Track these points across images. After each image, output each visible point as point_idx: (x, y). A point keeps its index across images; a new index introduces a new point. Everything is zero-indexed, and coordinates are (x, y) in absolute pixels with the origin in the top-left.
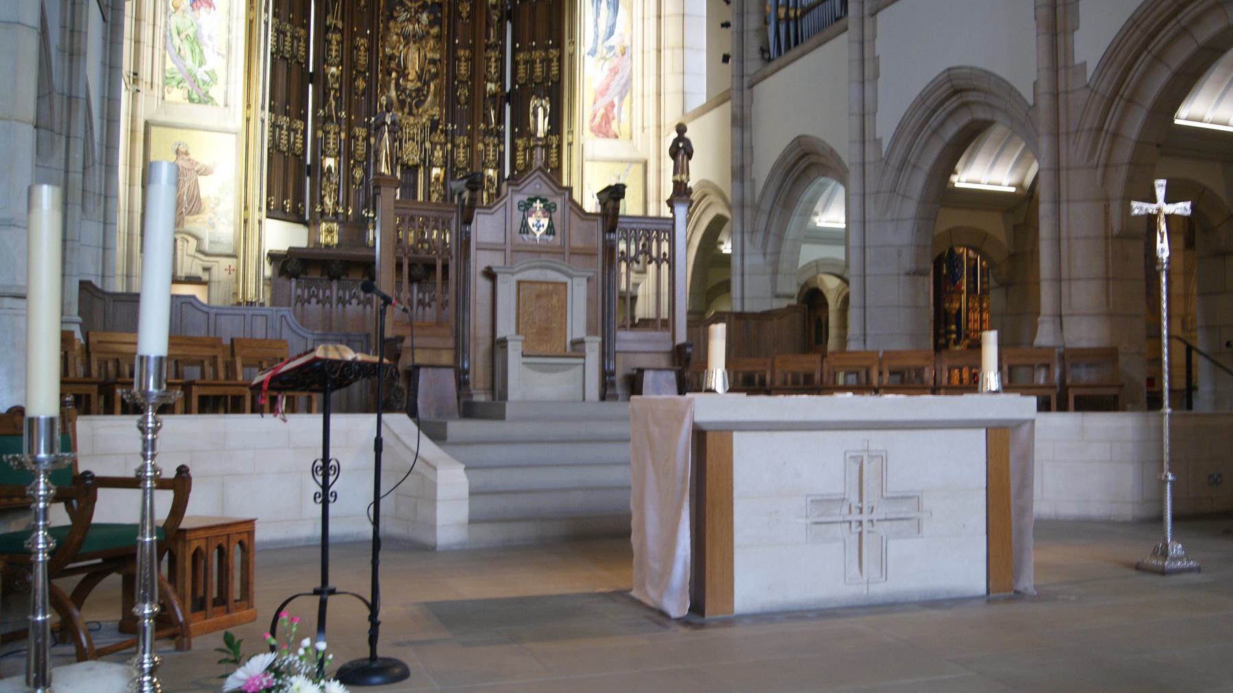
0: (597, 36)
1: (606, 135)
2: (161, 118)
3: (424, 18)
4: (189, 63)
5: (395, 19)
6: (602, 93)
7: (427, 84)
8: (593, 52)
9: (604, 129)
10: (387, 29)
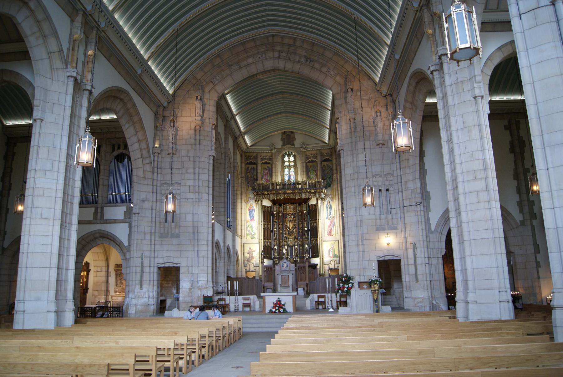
0: (327, 215)
1: (331, 236)
2: (246, 242)
3: (292, 217)
4: (251, 231)
5: (287, 218)
6: (329, 226)
7: (293, 230)
8: (327, 219)
9: (330, 234)
10: (285, 220)
